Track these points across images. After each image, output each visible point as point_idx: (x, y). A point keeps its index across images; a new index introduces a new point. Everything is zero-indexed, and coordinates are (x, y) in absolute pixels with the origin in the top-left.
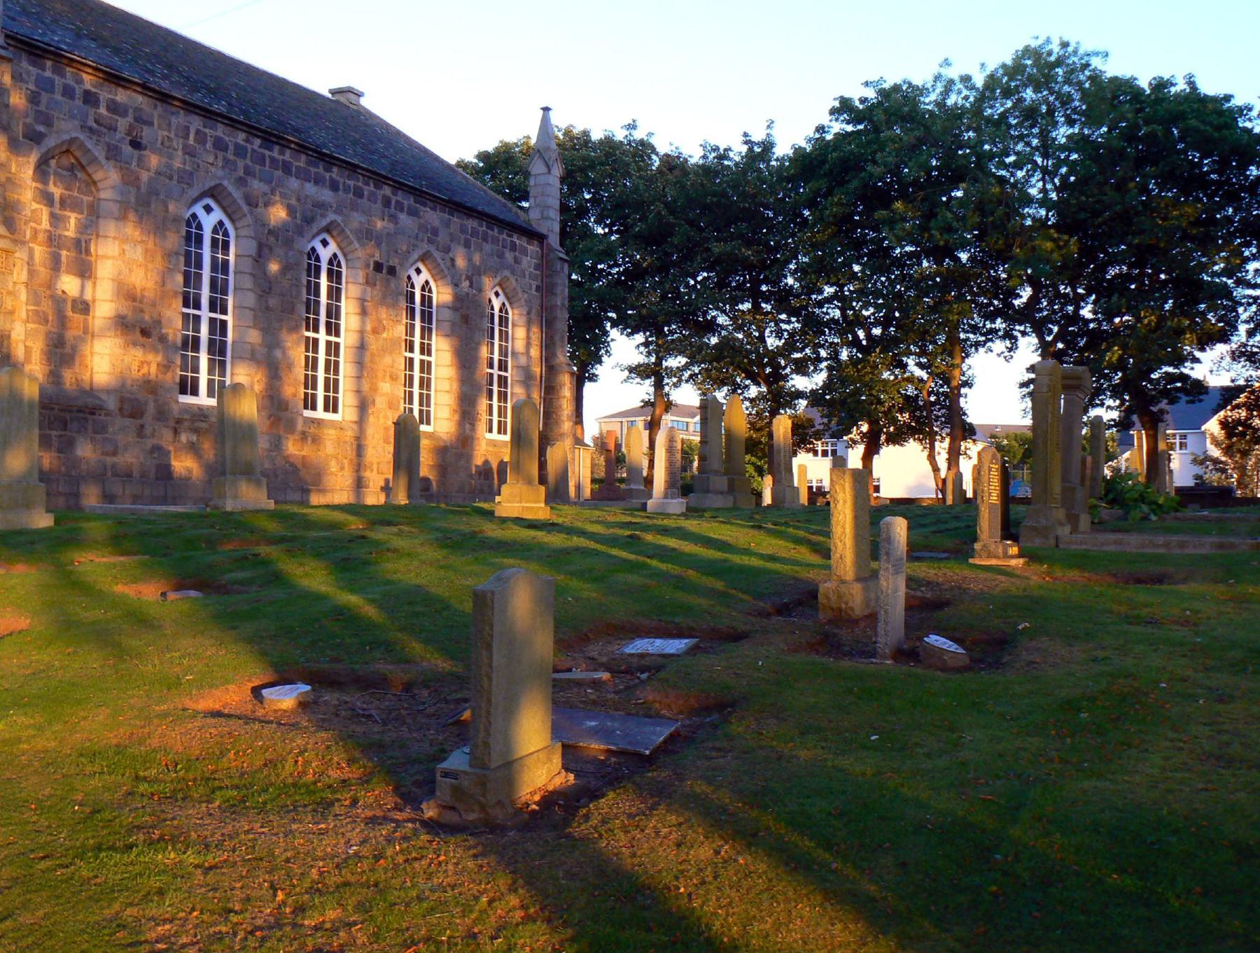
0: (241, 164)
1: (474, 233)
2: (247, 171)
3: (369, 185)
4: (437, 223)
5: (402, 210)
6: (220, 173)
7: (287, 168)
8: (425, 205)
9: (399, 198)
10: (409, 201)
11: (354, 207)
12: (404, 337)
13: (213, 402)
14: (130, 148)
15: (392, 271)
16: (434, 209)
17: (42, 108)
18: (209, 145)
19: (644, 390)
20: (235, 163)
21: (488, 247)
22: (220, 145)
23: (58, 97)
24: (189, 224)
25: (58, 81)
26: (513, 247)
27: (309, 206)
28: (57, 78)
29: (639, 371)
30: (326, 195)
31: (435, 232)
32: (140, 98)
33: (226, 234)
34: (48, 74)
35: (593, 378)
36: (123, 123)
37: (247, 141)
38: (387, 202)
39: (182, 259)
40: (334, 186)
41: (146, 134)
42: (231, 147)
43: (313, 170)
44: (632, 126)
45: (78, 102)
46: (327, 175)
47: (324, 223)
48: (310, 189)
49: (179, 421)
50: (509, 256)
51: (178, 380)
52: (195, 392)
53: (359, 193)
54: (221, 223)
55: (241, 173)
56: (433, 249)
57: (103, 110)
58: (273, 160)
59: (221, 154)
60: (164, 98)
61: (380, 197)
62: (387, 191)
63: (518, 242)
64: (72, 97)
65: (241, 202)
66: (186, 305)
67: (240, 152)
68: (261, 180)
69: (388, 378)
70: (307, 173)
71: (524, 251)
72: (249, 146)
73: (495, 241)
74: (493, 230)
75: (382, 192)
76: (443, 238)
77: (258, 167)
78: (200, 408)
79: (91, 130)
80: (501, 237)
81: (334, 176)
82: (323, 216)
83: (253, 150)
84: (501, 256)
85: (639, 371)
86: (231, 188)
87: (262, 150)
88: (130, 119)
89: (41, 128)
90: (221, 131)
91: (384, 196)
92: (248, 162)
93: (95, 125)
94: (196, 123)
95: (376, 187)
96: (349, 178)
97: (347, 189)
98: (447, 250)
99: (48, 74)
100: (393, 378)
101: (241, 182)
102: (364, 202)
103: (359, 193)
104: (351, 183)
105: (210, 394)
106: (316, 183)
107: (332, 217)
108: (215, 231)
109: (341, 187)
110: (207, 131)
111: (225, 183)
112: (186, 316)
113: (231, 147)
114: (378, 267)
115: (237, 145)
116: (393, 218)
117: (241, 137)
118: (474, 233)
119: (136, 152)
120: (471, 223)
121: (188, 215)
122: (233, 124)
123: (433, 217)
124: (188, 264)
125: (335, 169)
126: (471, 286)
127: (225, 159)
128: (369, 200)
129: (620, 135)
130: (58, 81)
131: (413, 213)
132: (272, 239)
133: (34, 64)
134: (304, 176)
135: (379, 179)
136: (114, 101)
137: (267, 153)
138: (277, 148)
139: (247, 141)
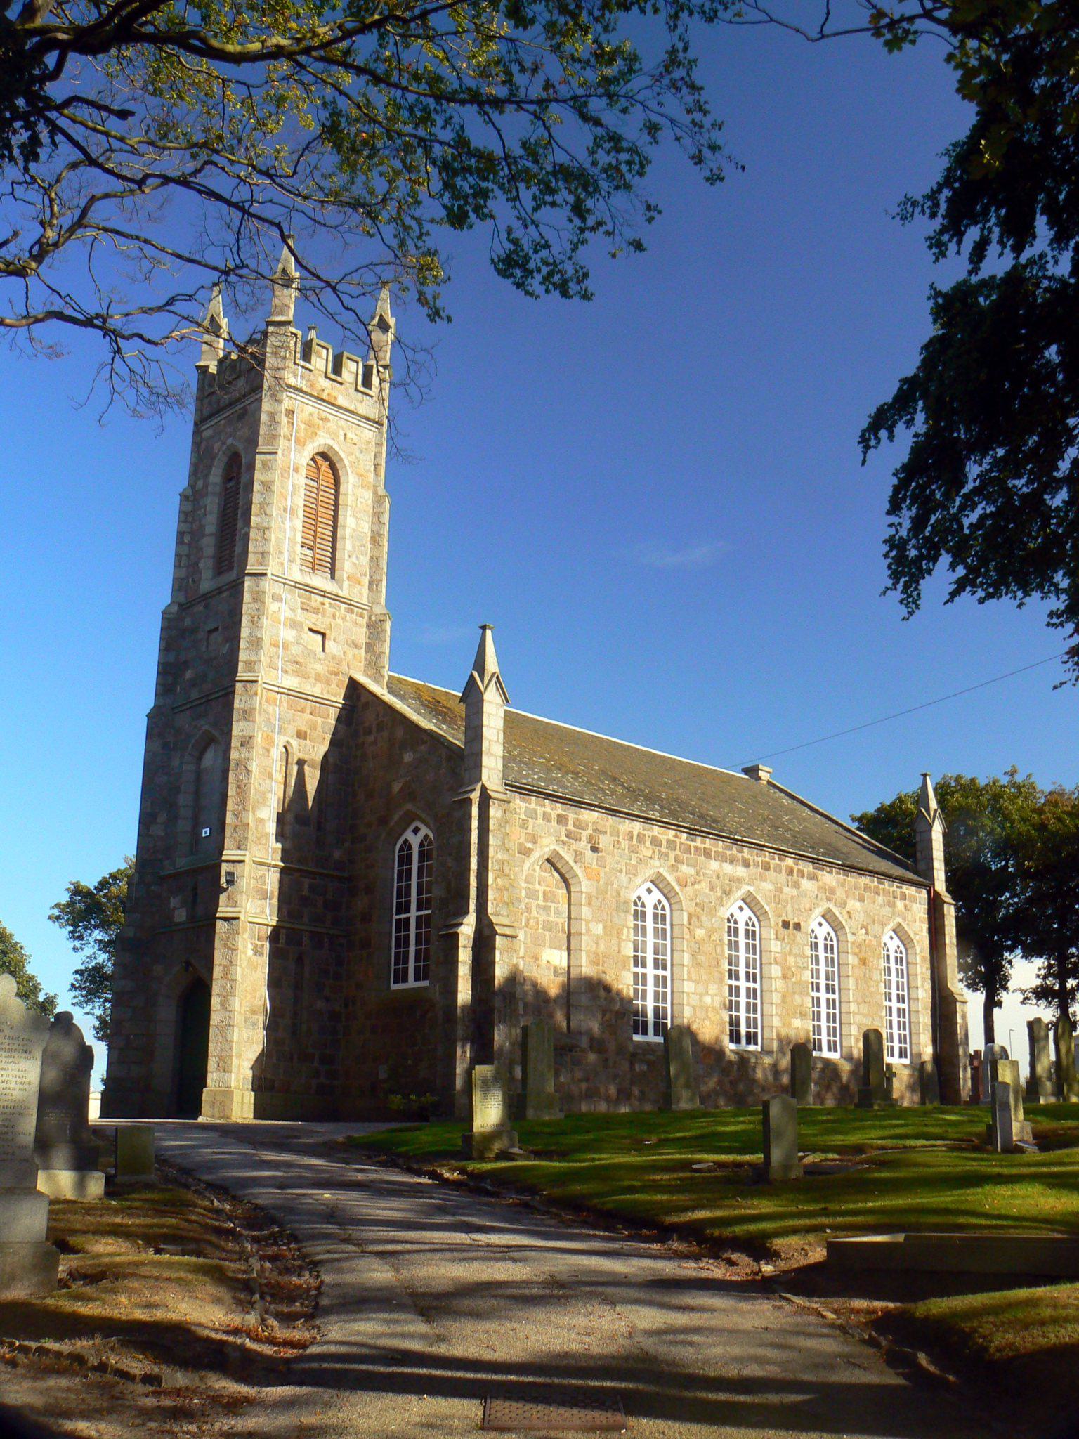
0: (672, 855)
1: (867, 888)
2: (677, 859)
3: (774, 859)
4: (834, 884)
5: (803, 876)
6: (657, 863)
7: (707, 854)
8: (823, 870)
9: (800, 867)
10: (808, 868)
11: (763, 878)
12: (810, 980)
13: (660, 1040)
14: (590, 852)
15: (797, 926)
16: (831, 872)
17: (530, 831)
18: (648, 843)
19: (1048, 1014)
20: (667, 855)
21: (880, 899)
22: (656, 842)
23: (540, 821)
24: (635, 904)
25: (540, 810)
26: (904, 896)
27: (727, 881)
28: (539, 808)
29: (1042, 993)
30: (741, 871)
31: (832, 891)
32: (596, 814)
33: (663, 909)
34: (533, 806)
35: (999, 1004)
36: (585, 834)
37: (676, 836)
38: (790, 872)
39: (632, 931)
40: (746, 864)
41: (604, 842)
42: (664, 843)
43: (728, 853)
44: (1013, 772)
45: (554, 823)
46: (740, 855)
47: (740, 893)
48: (728, 868)
49: (634, 1055)
50: (900, 905)
51: (632, 1023)
52: (645, 1033)
53: (766, 867)
54: (659, 902)
55: (672, 861)
56: (831, 906)
57: (571, 827)
58: (696, 849)
59: (657, 849)
60: (613, 812)
61: (784, 868)
62: (790, 862)
63: (907, 892)
64: (549, 821)
65: (674, 884)
66: (636, 964)
67: (671, 845)
68: (688, 865)
69: (798, 1015)
70: (724, 855)
71: (914, 900)
72: (678, 840)
73: (886, 893)
74: (883, 884)
75: (785, 864)
76: (840, 893)
77: (685, 856)
78: (648, 1044)
79: (563, 842)
80: (891, 889)
81: (745, 855)
82: (739, 888)
83: (681, 843)
84: (892, 905)
85: (1042, 993)
86: (666, 874)
87: (689, 842)
88: (590, 831)
89: (530, 845)
90: (656, 831)
91: (787, 866)
92: (678, 852)
93: (565, 839)
94: (637, 827)
95: (780, 860)
96: (757, 855)
97: (756, 865)
98: (844, 904)
99: (533, 806)
100: (803, 1015)
101: (674, 868)
102: (771, 873)
103: (766, 867)
104: (759, 859)
105: (656, 1033)
106: (732, 862)
107: (746, 888)
108: (655, 907)
109: (752, 864)
110: (645, 832)
111: (661, 870)
112: (636, 975)
113: (664, 843)
114: (786, 925)
115: (668, 841)
116: (797, 885)
117: (671, 834)
118: (867, 888)
119: (596, 855)
120: (864, 880)
121: (634, 897)
122: (665, 824)
123: (830, 878)
124: (636, 934)
125: (746, 850)
126: (867, 933)
127: (660, 852)
128: (775, 871)
129: (1004, 780)
130: (540, 810)
131: (813, 878)
132: (698, 910)
133: (524, 801)
134: (722, 858)
135: (782, 853)
136: (578, 819)
137: (692, 844)
138: (699, 839)
139: (676, 836)
